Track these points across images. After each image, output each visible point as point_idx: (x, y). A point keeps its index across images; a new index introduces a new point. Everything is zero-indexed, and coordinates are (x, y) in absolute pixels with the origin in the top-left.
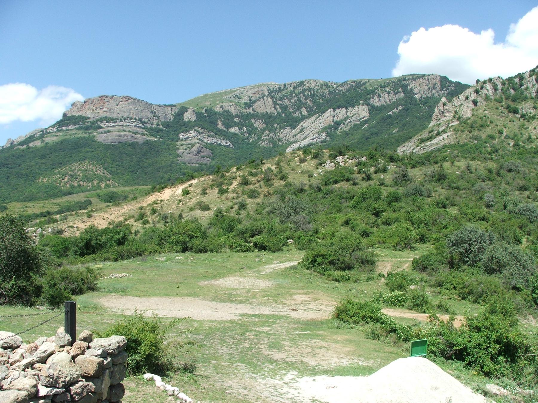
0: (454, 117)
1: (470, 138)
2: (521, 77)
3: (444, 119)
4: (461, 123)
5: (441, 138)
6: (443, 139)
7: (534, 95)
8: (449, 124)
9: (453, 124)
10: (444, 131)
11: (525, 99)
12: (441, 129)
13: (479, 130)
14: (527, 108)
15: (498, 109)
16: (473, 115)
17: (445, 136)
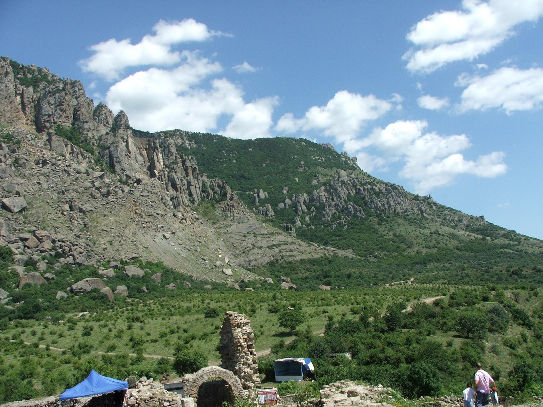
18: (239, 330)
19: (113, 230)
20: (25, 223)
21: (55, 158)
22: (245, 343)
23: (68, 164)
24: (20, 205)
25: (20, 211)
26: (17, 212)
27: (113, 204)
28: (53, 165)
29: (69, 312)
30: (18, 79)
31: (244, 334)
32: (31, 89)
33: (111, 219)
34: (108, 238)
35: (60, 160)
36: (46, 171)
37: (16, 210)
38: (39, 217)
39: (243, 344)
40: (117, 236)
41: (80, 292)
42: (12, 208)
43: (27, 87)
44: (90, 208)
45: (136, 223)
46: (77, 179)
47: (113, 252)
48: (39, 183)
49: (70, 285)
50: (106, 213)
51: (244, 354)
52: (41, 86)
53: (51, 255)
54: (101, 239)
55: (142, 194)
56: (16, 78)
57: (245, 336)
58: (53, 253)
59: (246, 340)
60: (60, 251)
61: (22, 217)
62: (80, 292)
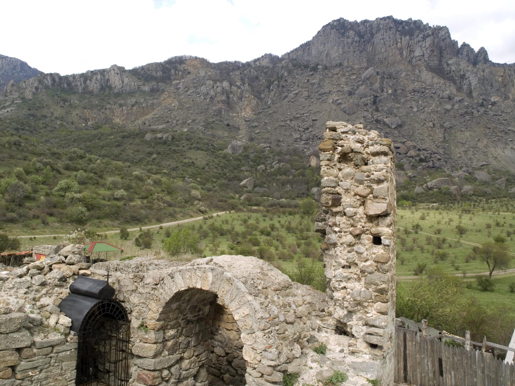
0: (19, 97)
1: (29, 115)
2: (74, 76)
3: (11, 96)
4: (23, 102)
5: (6, 110)
6: (8, 111)
7: (80, 91)
8: (13, 101)
9: (17, 102)
10: (8, 106)
11: (74, 93)
12: (7, 104)
13: (37, 110)
14: (75, 100)
15: (53, 96)
16: (34, 98)
17: (9, 109)
18: (348, 169)
19: (467, 143)
20: (399, 136)
21: (424, 88)
22: (361, 210)
23: (434, 92)
24: (396, 123)
25: (396, 127)
26: (394, 128)
27: (470, 122)
28: (422, 93)
29: (423, 202)
30: (399, 31)
31: (361, 182)
32: (407, 37)
33: (467, 134)
34: (464, 149)
35: (428, 89)
36: (416, 98)
37: (393, 127)
38: (409, 132)
39: (349, 210)
40: (471, 147)
41: (434, 188)
42: (390, 125)
43: (405, 36)
44: (450, 125)
45: (488, 137)
46: (440, 103)
47: (466, 160)
48: (411, 107)
49: (426, 183)
50: (463, 129)
51: (349, 238)
52: (416, 35)
53: (416, 160)
54: (457, 150)
55: (495, 114)
56: (397, 30)
57: (362, 189)
58: (418, 158)
59: (363, 200)
60: (423, 157)
61: (397, 132)
62: (434, 188)
